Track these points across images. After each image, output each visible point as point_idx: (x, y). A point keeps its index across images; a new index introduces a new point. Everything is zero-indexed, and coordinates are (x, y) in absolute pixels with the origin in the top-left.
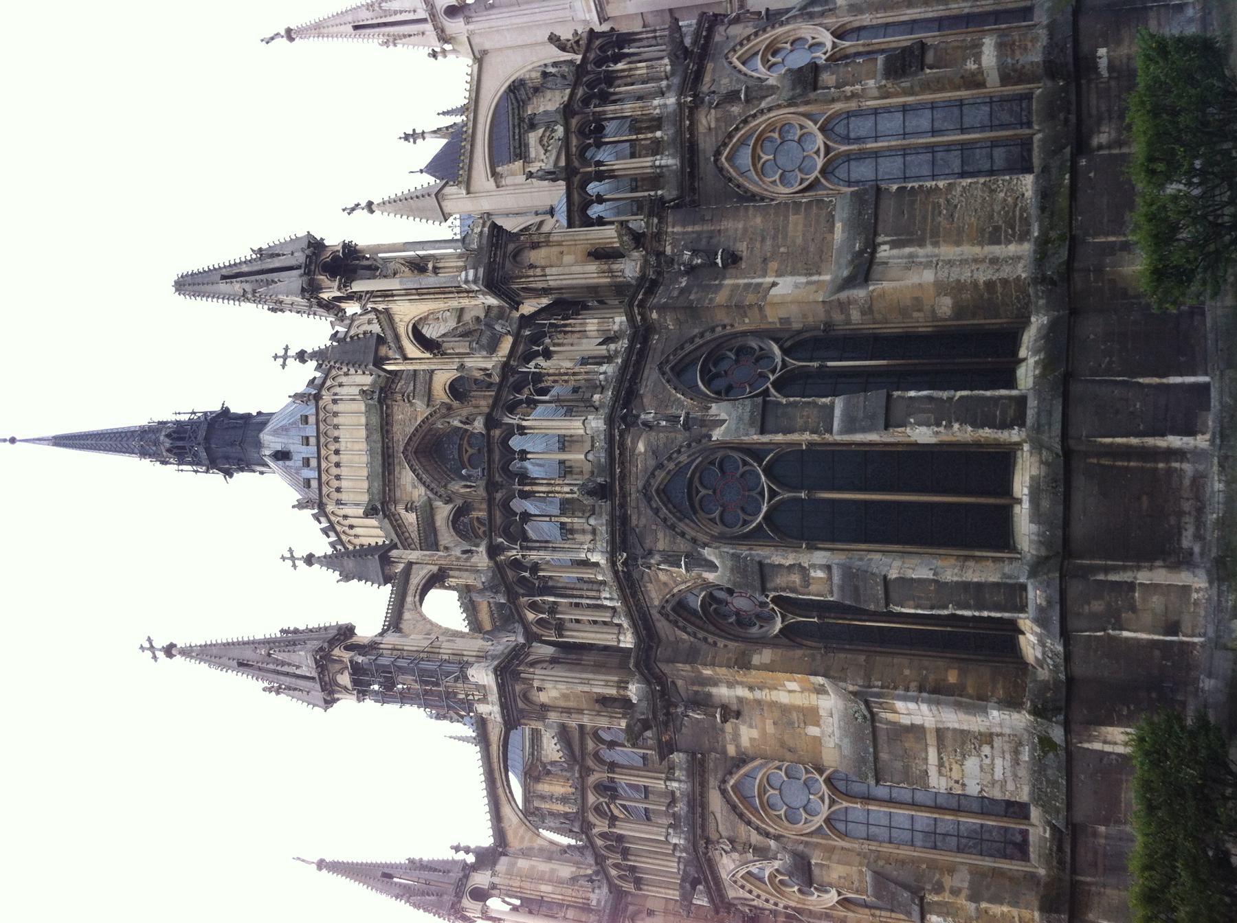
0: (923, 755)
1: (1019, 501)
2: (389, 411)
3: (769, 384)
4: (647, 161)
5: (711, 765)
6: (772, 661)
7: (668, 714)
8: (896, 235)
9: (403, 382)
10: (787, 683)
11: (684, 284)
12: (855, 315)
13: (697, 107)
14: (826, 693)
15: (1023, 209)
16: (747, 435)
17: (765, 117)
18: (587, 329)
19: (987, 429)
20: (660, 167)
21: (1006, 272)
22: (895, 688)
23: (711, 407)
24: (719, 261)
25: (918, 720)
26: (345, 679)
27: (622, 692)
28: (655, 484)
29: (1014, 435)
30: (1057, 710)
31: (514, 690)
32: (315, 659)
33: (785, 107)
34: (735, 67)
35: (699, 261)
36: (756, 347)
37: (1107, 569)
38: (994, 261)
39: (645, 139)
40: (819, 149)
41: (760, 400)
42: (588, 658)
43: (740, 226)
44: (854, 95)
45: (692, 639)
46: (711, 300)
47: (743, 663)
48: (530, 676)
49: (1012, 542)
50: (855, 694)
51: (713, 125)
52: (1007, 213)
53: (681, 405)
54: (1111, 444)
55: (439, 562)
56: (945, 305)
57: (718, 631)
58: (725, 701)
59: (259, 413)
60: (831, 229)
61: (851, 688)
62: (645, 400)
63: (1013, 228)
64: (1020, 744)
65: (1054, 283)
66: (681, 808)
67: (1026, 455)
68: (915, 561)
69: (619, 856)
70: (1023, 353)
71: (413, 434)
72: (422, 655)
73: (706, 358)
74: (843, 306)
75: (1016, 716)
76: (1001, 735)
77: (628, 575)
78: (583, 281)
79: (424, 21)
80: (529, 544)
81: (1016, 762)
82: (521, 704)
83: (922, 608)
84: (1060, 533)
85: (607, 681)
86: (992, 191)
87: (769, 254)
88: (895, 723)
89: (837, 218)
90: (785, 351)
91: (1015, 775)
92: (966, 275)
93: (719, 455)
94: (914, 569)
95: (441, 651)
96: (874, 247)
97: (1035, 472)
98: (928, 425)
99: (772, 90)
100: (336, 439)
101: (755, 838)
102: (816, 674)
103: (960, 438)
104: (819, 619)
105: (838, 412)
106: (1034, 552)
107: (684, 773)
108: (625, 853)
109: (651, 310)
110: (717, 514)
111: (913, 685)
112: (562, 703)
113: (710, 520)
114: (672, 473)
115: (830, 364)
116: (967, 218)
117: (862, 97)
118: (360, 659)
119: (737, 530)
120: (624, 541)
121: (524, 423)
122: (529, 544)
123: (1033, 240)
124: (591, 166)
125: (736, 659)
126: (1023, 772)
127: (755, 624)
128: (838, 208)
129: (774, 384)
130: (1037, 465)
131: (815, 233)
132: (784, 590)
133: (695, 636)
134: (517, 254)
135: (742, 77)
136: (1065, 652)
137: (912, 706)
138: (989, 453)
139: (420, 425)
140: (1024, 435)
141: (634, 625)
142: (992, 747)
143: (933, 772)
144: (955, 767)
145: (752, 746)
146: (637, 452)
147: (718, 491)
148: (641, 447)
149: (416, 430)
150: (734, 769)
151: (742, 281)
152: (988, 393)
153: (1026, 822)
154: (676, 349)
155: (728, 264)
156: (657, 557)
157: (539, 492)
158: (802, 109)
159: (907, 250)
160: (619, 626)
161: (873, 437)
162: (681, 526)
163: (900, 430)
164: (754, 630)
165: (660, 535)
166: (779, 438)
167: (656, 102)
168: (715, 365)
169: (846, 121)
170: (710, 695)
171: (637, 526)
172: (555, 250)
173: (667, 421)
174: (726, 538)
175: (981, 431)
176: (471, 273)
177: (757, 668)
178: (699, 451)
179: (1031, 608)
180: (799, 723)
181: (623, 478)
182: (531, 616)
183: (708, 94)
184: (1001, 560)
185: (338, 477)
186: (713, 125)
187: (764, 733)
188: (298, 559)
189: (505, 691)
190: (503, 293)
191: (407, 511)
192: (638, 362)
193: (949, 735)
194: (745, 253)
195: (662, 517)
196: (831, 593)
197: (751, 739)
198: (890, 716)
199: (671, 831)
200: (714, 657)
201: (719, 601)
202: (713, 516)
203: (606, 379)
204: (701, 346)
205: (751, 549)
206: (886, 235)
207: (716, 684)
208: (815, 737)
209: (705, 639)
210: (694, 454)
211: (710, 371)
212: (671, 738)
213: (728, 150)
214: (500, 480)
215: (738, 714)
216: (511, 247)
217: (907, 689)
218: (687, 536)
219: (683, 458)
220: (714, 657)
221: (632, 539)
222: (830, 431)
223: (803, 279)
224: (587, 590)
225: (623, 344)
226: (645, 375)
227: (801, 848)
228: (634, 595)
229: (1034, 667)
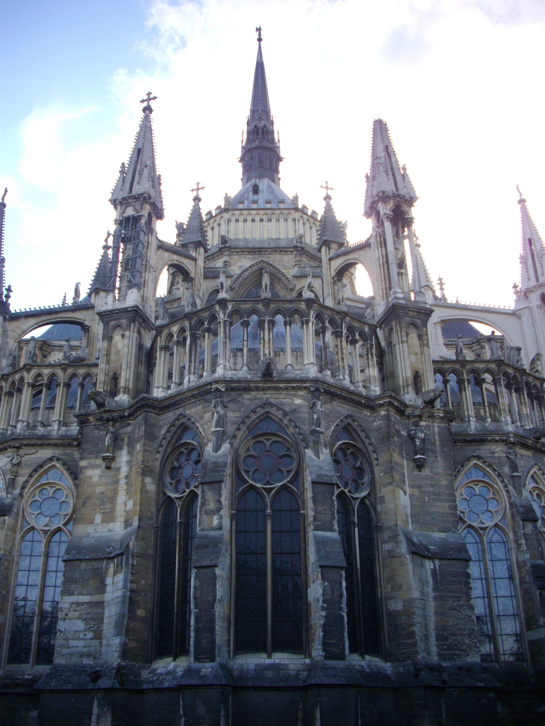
0: (85, 592)
1: (269, 657)
2: (289, 253)
3: (342, 488)
4: (472, 412)
5: (69, 451)
6: (147, 491)
7: (108, 420)
8: (440, 572)
9: (307, 262)
10: (132, 501)
11: (402, 433)
12: (388, 546)
13: (507, 444)
14: (126, 527)
16: (311, 473)
17: (502, 489)
18: (371, 369)
19: (322, 634)
20: (469, 421)
21: (421, 645)
22: (132, 574)
23: (326, 449)
24: (418, 456)
25: (109, 589)
26: (130, 212)
27: (122, 390)
28: (273, 410)
29: (317, 651)
30: (122, 683)
31: (122, 318)
32: (144, 194)
33: (509, 501)
34: (530, 470)
35: (418, 443)
36: (364, 480)
37: (226, 716)
38: (426, 637)
39: (485, 411)
40: (483, 523)
41: (334, 482)
42: (143, 369)
43: (440, 471)
44: (519, 545)
45: (161, 437)
46: (394, 450)
47: (146, 471)
48: (132, 330)
49: (241, 652)
50: (128, 546)
51: (496, 455)
52: (456, 645)
53: (328, 428)
54: (315, 718)
55: (196, 279)
56: (397, 606)
57: (167, 454)
58: (117, 459)
59: (279, 179)
61: (131, 544)
62: (329, 404)
63: (445, 650)
64: (95, 658)
65: (416, 676)
66: (41, 430)
67: (302, 661)
68: (227, 588)
69: (8, 390)
70: (367, 657)
71: (274, 267)
72: (145, 260)
73: (355, 445)
74: (394, 538)
75: (116, 655)
76: (101, 645)
77: (209, 392)
78: (399, 367)
79: (537, 280)
80: (228, 327)
81: (82, 655)
82: (112, 323)
83: (194, 591)
84: (251, 684)
85: (129, 380)
86: (469, 635)
87: (423, 489)
88: (106, 573)
89: (448, 534)
90: (362, 500)
91: (72, 654)
92: (417, 619)
93: (294, 454)
94: (222, 586)
95: (147, 273)
97: (291, 667)
98: (323, 595)
99: (520, 493)
100: (270, 220)
101: (21, 480)
102: (140, 520)
103: (313, 616)
104: (180, 523)
105: (328, 534)
106: (235, 667)
107: (64, 433)
108: (10, 394)
109: (387, 410)
110: (252, 453)
111: (134, 586)
112: (113, 350)
113: (248, 448)
114: (280, 422)
115: (356, 529)
117: (518, 551)
118: (143, 221)
119: (242, 467)
120: (233, 389)
121: (310, 324)
122: (228, 327)
123: (440, 662)
124: (467, 376)
125: (148, 467)
126: (75, 660)
127: (172, 480)
128: (454, 535)
129: (342, 492)
130: (296, 668)
132: (203, 497)
133: (164, 438)
134: (414, 325)
135: (525, 474)
136: (163, 688)
137: (121, 585)
138: (302, 636)
139: (280, 271)
140: (319, 659)
141: (171, 397)
142: (92, 639)
143: (74, 599)
144: (77, 614)
145: (87, 477)
146: (294, 398)
147: (268, 453)
148: (298, 401)
149: (277, 269)
150: (66, 467)
151: (406, 471)
152: (346, 635)
153: (35, 662)
154: (361, 426)
155: (416, 462)
156: (222, 412)
157: (264, 333)
158: (508, 512)
159: (430, 580)
160: (169, 388)
161: (312, 557)
162: (244, 428)
163: (320, 575)
164: (168, 479)
165: (237, 414)
166: (309, 494)
167: (509, 418)
168: (352, 453)
169: (501, 540)
170: (121, 448)
171: (243, 398)
172: (418, 350)
173: (317, 419)
174: (236, 459)
175: (321, 630)
176: (401, 296)
177: (143, 481)
178: (296, 441)
179: (198, 665)
180: (103, 509)
181: (276, 389)
182: (175, 329)
183: (515, 452)
184: (229, 645)
185: (245, 221)
186: (496, 455)
187: (96, 485)
188: (198, 192)
189: (122, 312)
190: (388, 316)
191: (224, 262)
192: (353, 401)
193: (99, 610)
194: (424, 474)
195: (250, 415)
196: (202, 530)
197: (91, 476)
198: (111, 570)
199: (25, 424)
200: (149, 451)
201: (189, 455)
202: (251, 450)
203: (339, 380)
204: (364, 444)
205: (230, 475)
206: (440, 566)
207: (129, 453)
208: (94, 519)
209: (161, 446)
210: (295, 437)
211: (348, 449)
212: (91, 422)
213: (481, 464)
214: (271, 308)
215: (108, 468)
216: (418, 322)
217: (132, 582)
218: (237, 432)
219: (291, 430)
220: (149, 451)
221: (233, 394)
222: (316, 529)
223: (409, 512)
224: (195, 366)
225: (364, 392)
226: (344, 406)
227: (15, 510)
228: (194, 396)
229: (149, 667)
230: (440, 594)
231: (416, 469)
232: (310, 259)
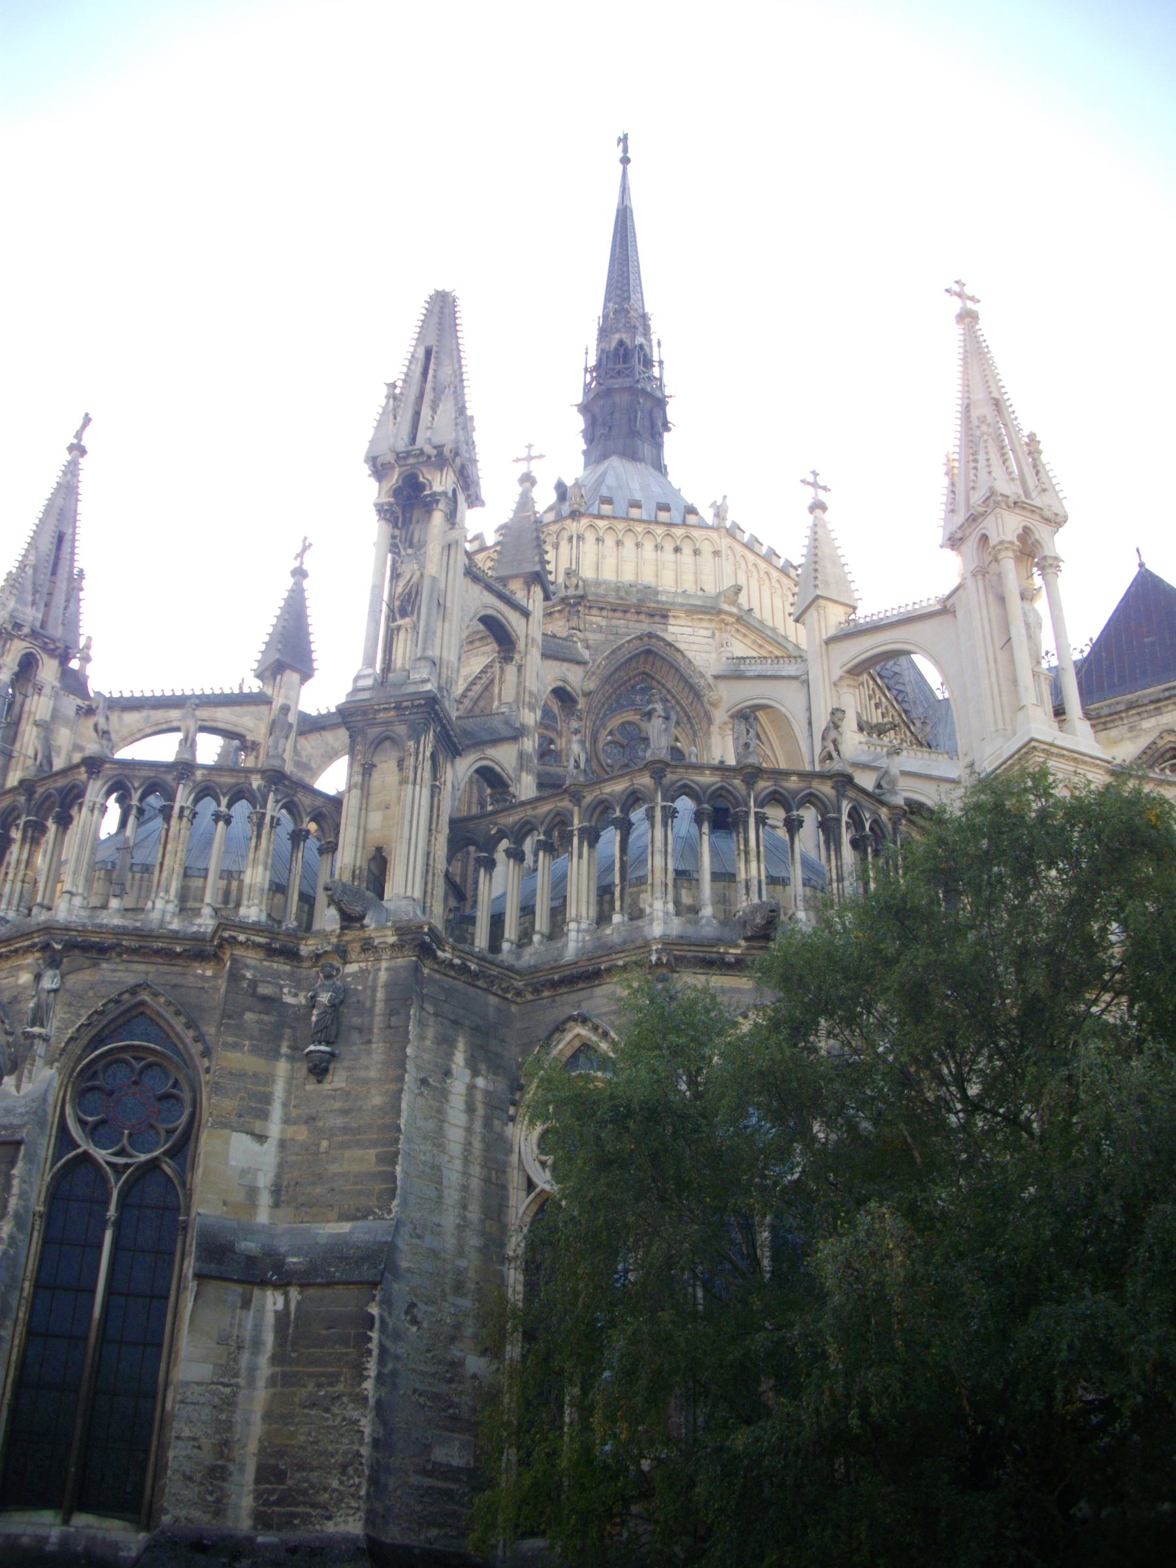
2: (557, 615)
8: (297, 1318)
9: (603, 623)
15: (305, 1519)
43: (373, 1074)
52: (304, 1493)
60: (344, 1217)
63: (277, 1503)
86: (344, 1468)
87: (320, 1124)
89: (359, 1223)
96: (282, 1285)
116: (305, 1429)
131: (342, 1192)
159: (269, 1338)
230: (287, 1369)
231: (313, 1079)
232: (611, 614)
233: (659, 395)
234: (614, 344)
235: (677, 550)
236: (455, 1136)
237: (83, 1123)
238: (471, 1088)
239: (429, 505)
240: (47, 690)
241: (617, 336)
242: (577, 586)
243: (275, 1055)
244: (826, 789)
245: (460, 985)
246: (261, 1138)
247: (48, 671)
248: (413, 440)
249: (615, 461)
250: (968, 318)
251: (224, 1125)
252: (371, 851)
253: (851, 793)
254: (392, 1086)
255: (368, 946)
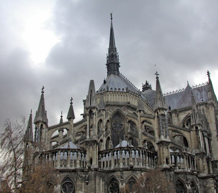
43: (93, 184)
233: (118, 63)
234: (111, 54)
235: (121, 96)
236: (101, 189)
237: (63, 190)
238: (102, 184)
239: (93, 114)
240: (44, 129)
241: (112, 53)
242: (108, 103)
243: (83, 182)
244: (139, 149)
245: (101, 173)
246: (82, 191)
247: (44, 126)
248: (91, 106)
249: (112, 76)
250: (157, 78)
251: (78, 190)
252: (90, 158)
253: (141, 149)
254: (95, 185)
255: (91, 170)
